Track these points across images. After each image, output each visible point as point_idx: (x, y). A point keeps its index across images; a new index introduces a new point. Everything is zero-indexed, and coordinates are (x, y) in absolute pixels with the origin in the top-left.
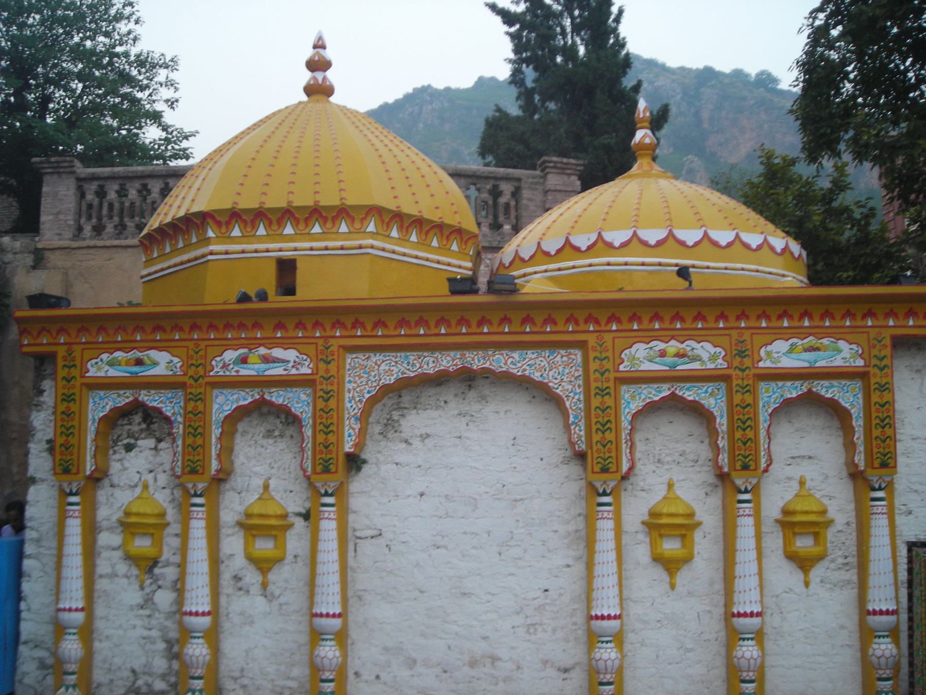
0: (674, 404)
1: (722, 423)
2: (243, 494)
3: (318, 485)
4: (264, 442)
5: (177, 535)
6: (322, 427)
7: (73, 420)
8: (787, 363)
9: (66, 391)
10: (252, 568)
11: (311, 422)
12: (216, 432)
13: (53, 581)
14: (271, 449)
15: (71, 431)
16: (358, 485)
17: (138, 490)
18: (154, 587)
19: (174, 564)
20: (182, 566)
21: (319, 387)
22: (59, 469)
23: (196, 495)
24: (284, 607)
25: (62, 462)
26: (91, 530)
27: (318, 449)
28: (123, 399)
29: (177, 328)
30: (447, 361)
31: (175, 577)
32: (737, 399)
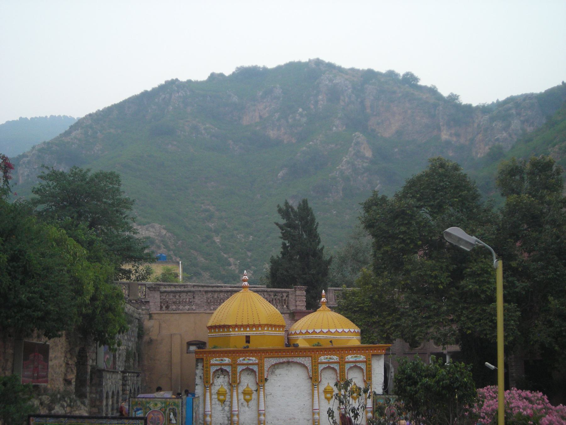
0: (329, 367)
1: (338, 371)
8: (351, 360)
12: (238, 374)
16: (266, 384)
20: (231, 402)
28: (218, 367)
29: (230, 353)
30: (285, 360)
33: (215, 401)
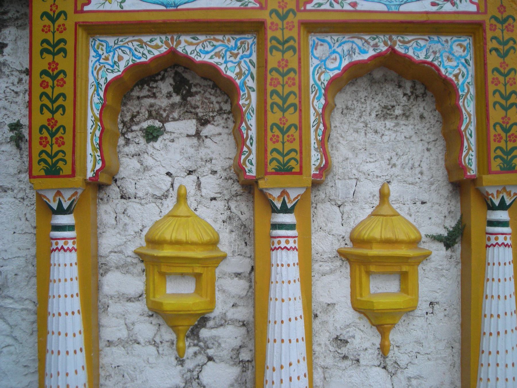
2: (347, 208)
3: (492, 191)
4: (379, 125)
5: (238, 275)
6: (497, 98)
7: (63, 83)
9: (49, 36)
10: (364, 323)
11: (472, 90)
13: (29, 351)
14: (390, 135)
15: (60, 101)
17: (170, 203)
18: (201, 359)
19: (233, 322)
20: (255, 330)
21: (489, 34)
22: (38, 169)
23: (284, 210)
24: (414, 382)
25: (44, 156)
26: (92, 270)
27: (492, 132)
28: (151, 49)
31: (237, 343)
33: (125, 319)
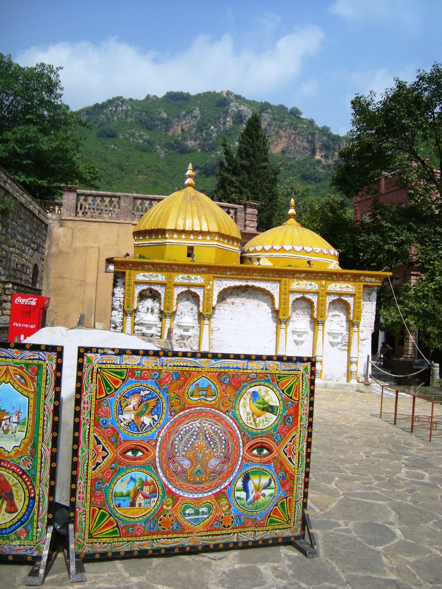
32: (321, 298)
